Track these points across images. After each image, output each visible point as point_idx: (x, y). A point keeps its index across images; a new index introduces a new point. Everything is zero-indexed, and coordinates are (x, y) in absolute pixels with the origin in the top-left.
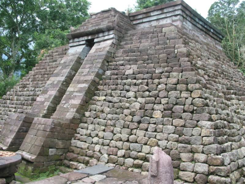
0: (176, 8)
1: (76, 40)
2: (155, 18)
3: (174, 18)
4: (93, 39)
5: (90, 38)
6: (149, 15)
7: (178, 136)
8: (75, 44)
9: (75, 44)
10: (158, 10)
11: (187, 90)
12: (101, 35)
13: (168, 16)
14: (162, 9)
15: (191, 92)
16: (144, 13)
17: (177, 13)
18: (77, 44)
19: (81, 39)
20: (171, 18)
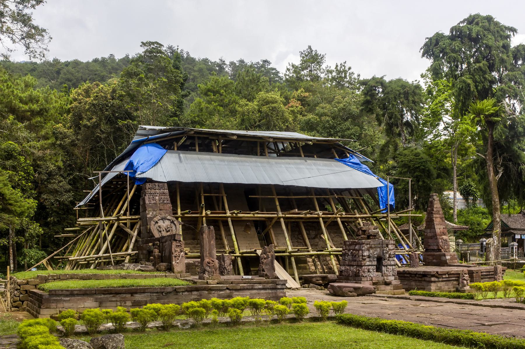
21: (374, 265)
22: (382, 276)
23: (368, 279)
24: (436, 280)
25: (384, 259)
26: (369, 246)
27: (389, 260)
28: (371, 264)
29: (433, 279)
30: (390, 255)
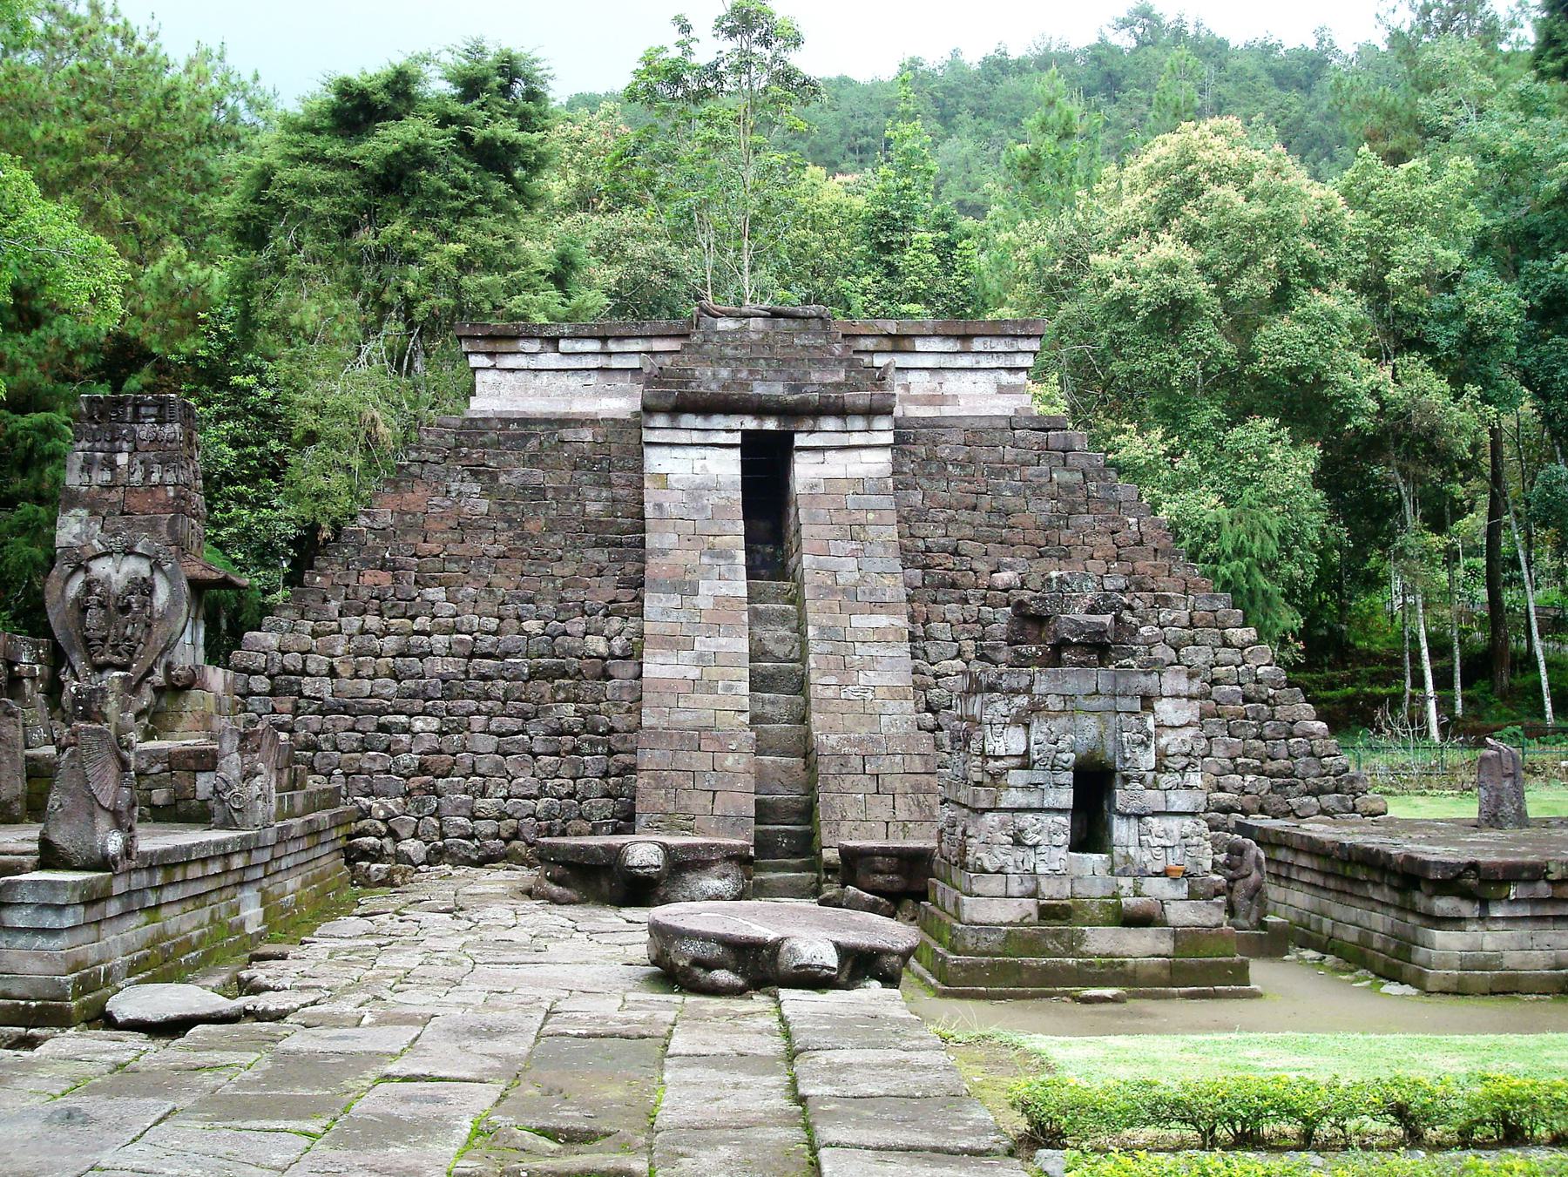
0: (1024, 345)
1: (688, 420)
2: (930, 361)
3: (1006, 378)
4: (789, 436)
5: (771, 425)
6: (907, 344)
7: (1257, 763)
8: (683, 437)
9: (683, 437)
10: (947, 336)
11: (1226, 644)
12: (830, 423)
13: (982, 365)
14: (966, 338)
15: (1242, 649)
16: (889, 336)
17: (1020, 361)
18: (696, 437)
19: (719, 421)
20: (992, 376)
21: (1060, 811)
22: (1111, 871)
23: (1015, 888)
24: (1467, 909)
25: (1126, 780)
26: (1022, 700)
27: (1155, 785)
28: (1033, 800)
29: (1444, 905)
30: (1162, 755)
